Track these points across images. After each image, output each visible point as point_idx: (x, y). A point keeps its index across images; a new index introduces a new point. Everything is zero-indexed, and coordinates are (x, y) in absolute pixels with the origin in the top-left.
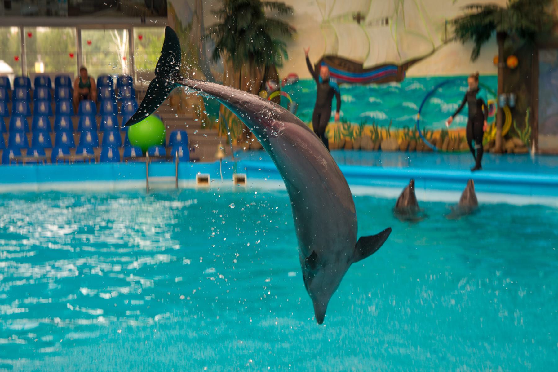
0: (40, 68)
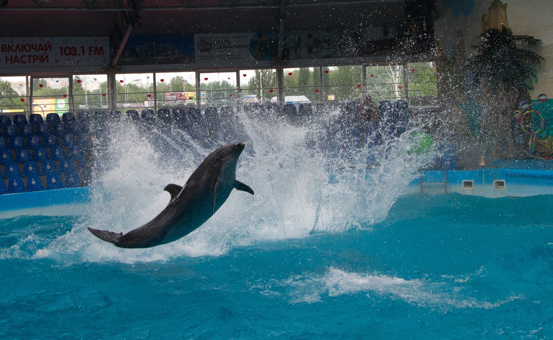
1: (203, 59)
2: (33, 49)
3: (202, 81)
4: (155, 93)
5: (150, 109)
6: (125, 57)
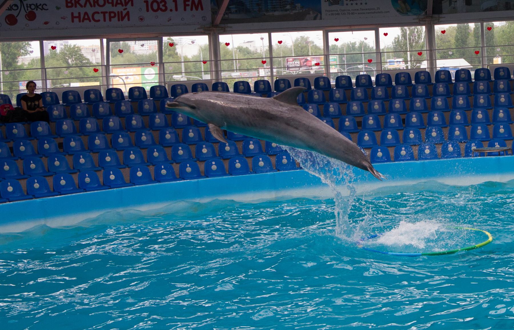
0: (498, 61)
1: (333, 14)
2: (109, 3)
3: (332, 42)
4: (271, 58)
5: (266, 79)
6: (231, 13)
